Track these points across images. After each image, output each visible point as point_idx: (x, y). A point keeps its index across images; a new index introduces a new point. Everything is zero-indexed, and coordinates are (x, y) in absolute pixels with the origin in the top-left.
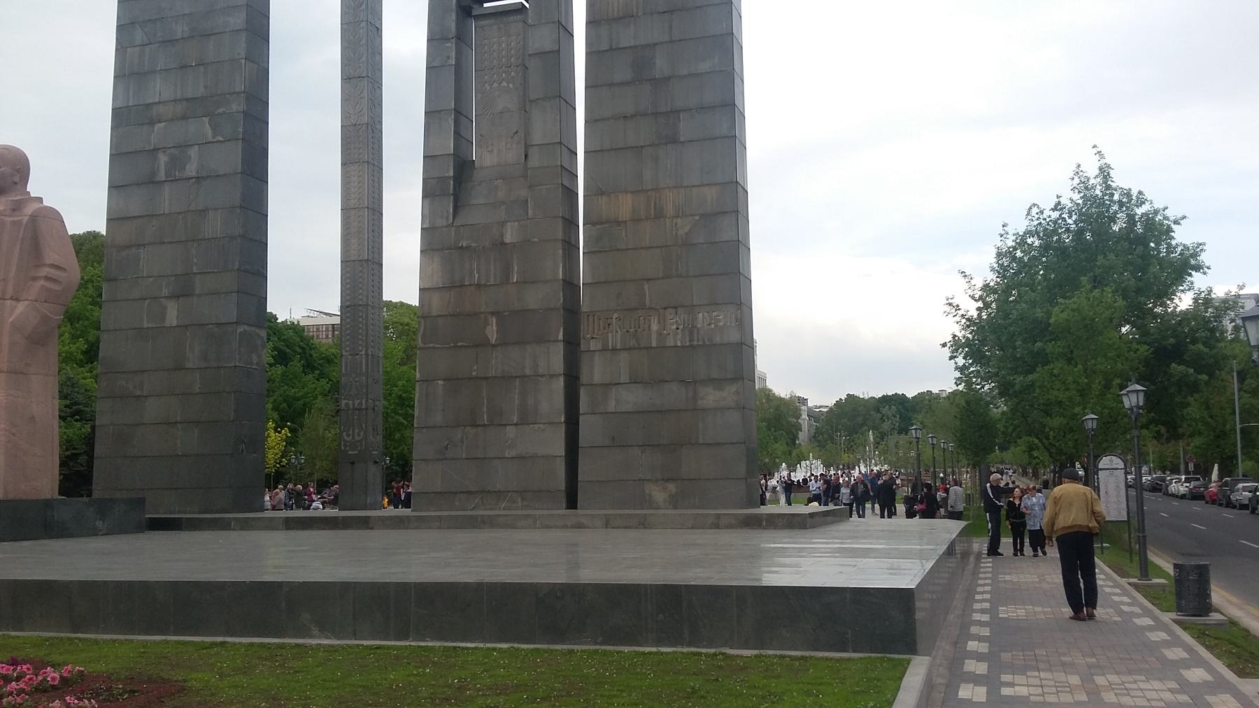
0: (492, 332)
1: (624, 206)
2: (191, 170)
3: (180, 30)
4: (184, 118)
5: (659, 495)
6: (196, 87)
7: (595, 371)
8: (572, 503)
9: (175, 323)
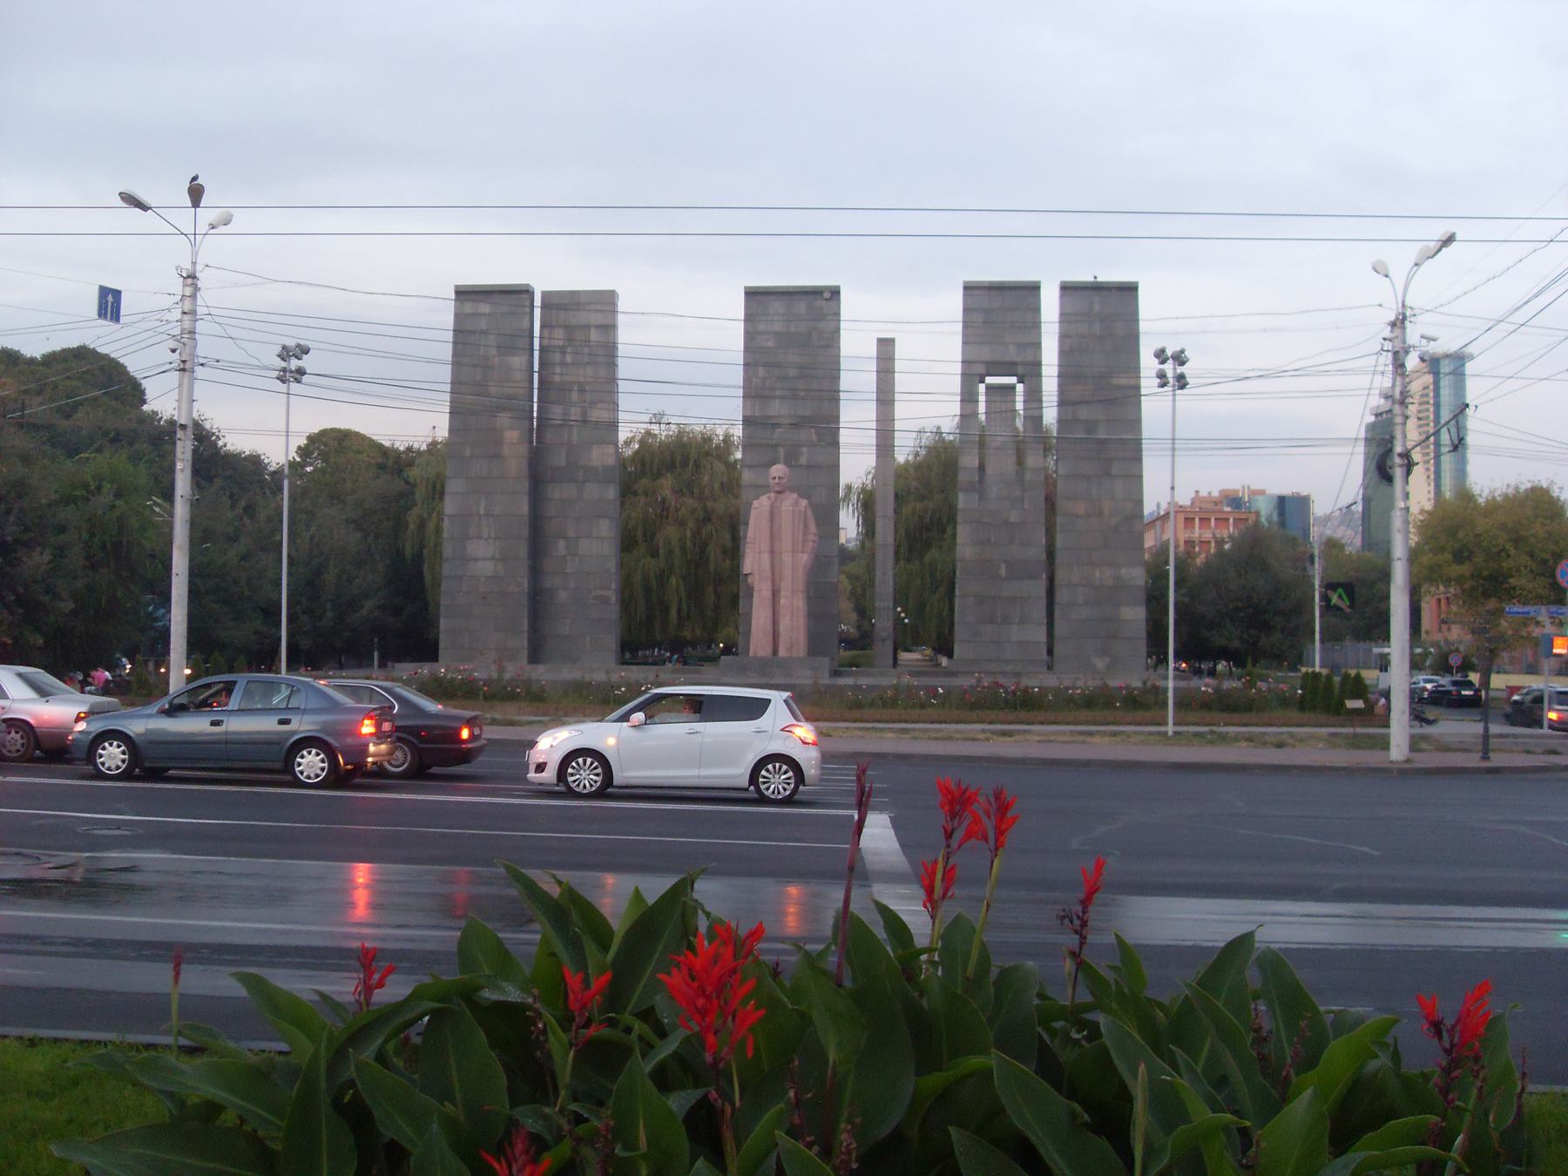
0: (1003, 572)
1: (1080, 507)
2: (803, 460)
5: (1100, 664)
6: (805, 409)
7: (1062, 596)
8: (1050, 667)
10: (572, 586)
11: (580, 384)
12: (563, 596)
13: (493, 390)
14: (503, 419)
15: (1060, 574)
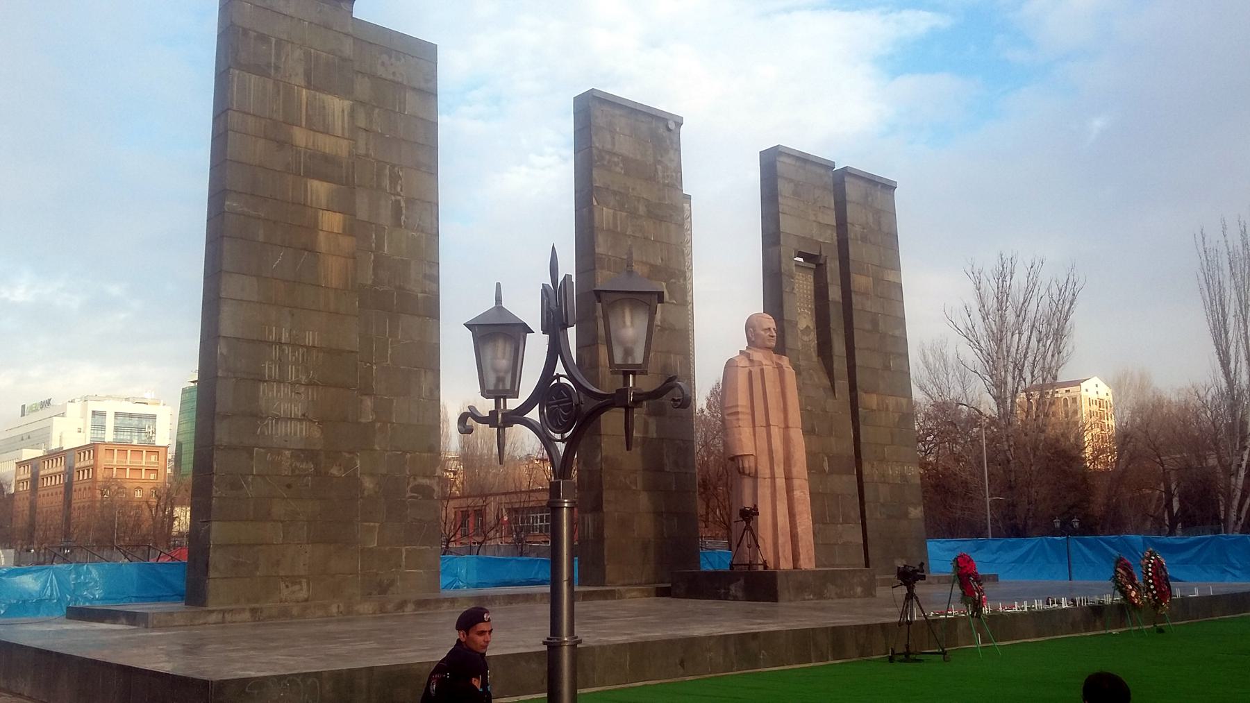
3: (642, 210)
4: (649, 277)
7: (868, 495)
9: (655, 435)
10: (384, 471)
11: (393, 166)
12: (368, 484)
13: (300, 136)
14: (319, 189)
15: (866, 469)
